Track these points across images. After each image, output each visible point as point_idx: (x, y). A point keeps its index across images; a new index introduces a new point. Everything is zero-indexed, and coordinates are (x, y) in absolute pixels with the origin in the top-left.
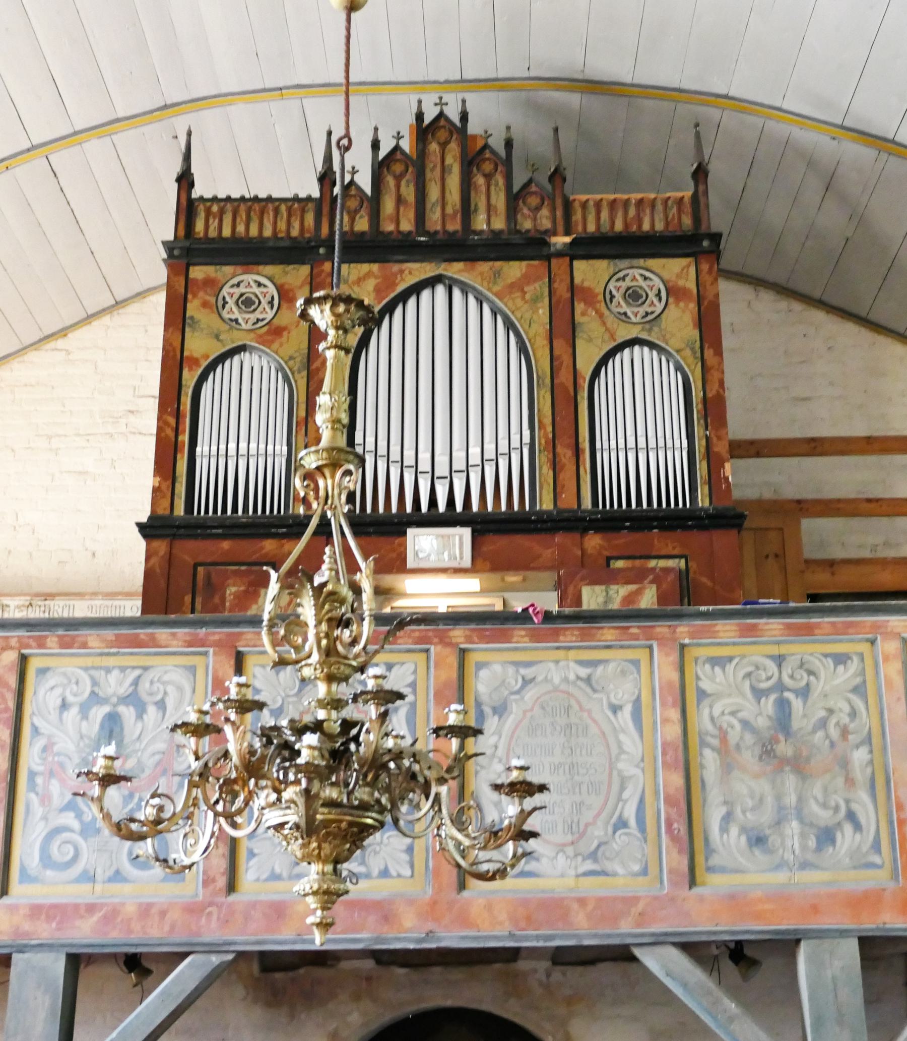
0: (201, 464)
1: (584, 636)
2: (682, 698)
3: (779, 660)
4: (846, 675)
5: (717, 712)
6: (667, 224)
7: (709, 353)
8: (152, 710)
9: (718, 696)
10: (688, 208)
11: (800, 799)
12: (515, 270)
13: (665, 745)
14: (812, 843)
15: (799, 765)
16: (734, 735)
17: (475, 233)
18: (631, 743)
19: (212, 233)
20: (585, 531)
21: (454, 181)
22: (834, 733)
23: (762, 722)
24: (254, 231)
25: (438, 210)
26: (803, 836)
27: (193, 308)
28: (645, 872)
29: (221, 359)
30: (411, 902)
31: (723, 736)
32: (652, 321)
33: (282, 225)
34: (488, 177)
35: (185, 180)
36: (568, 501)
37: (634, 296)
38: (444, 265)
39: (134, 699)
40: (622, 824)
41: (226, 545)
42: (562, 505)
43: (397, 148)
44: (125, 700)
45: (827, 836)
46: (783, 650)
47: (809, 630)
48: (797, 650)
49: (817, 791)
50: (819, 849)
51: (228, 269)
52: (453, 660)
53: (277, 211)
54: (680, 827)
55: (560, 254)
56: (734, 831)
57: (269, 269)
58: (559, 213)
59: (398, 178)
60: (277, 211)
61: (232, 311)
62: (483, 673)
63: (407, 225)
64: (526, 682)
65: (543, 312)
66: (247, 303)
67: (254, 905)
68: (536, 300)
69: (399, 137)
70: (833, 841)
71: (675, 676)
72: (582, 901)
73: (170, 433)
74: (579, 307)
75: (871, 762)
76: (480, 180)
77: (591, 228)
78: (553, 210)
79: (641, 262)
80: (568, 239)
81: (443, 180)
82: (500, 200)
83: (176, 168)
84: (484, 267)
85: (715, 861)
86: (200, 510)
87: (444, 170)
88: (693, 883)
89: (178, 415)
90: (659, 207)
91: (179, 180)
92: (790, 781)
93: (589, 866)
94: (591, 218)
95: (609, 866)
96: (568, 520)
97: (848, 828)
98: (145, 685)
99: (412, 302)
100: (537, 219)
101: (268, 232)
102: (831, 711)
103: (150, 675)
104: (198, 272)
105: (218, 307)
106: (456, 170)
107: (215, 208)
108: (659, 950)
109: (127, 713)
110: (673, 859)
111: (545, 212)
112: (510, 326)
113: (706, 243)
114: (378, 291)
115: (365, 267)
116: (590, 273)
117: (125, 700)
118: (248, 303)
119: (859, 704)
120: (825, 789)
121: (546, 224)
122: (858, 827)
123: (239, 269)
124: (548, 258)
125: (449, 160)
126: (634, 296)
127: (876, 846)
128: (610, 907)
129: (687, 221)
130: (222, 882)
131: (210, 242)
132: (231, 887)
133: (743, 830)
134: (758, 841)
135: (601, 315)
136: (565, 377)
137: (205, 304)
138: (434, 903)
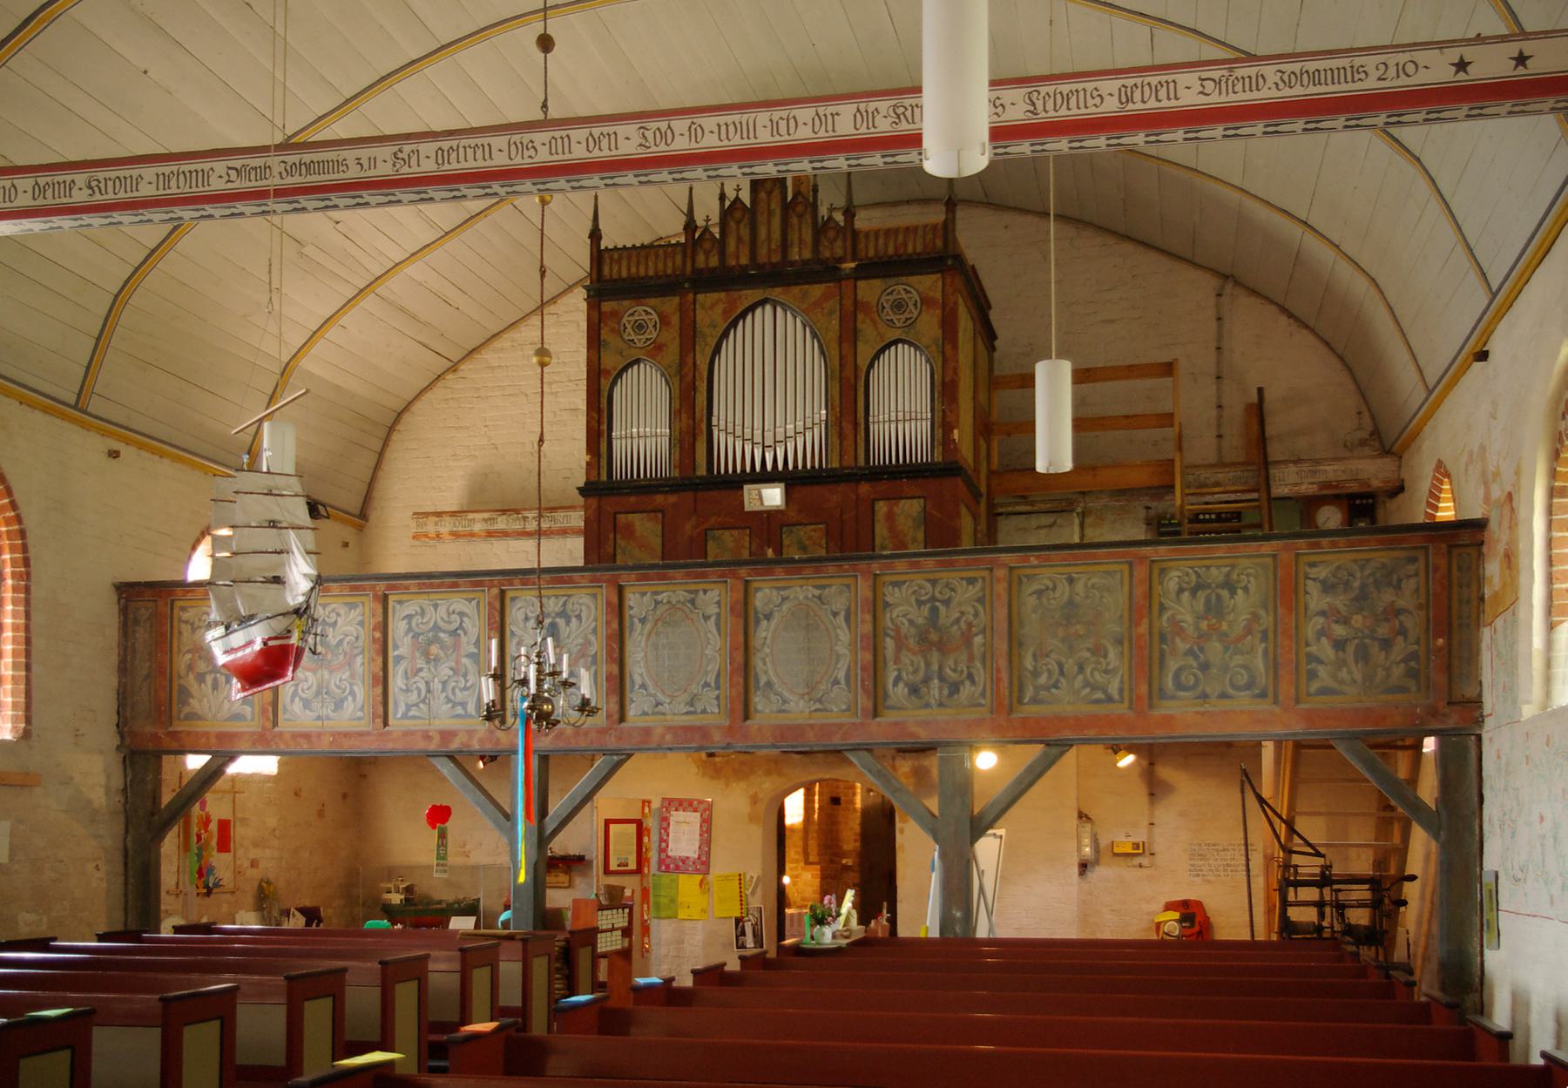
0: (616, 444)
1: (818, 570)
2: (876, 607)
3: (934, 582)
4: (973, 591)
5: (895, 614)
6: (925, 246)
7: (948, 347)
8: (574, 620)
9: (897, 605)
10: (940, 233)
11: (941, 668)
12: (817, 290)
13: (863, 636)
14: (946, 692)
15: (942, 647)
16: (904, 630)
17: (792, 264)
18: (844, 635)
19: (615, 276)
20: (858, 481)
21: (776, 222)
22: (963, 625)
23: (921, 621)
24: (642, 272)
25: (765, 246)
26: (941, 689)
27: (605, 334)
28: (848, 709)
29: (625, 369)
30: (718, 727)
31: (898, 630)
32: (910, 324)
33: (660, 266)
34: (800, 216)
35: (595, 235)
36: (849, 461)
37: (899, 306)
38: (769, 290)
39: (563, 614)
40: (836, 682)
41: (633, 499)
42: (845, 464)
43: (737, 198)
44: (559, 615)
45: (955, 688)
46: (937, 576)
47: (951, 564)
48: (945, 576)
49: (951, 663)
50: (951, 695)
51: (626, 303)
52: (741, 587)
53: (657, 256)
54: (869, 683)
55: (848, 277)
56: (901, 685)
57: (653, 301)
58: (849, 243)
59: (738, 223)
60: (657, 256)
61: (630, 334)
62: (759, 595)
63: (744, 260)
64: (784, 599)
65: (835, 322)
66: (640, 327)
67: (635, 729)
68: (831, 313)
69: (738, 190)
70: (958, 691)
71: (870, 594)
72: (812, 726)
73: (595, 424)
74: (860, 317)
75: (984, 645)
76: (795, 220)
77: (871, 253)
78: (845, 240)
79: (904, 279)
80: (853, 265)
81: (769, 222)
82: (808, 235)
83: (589, 225)
84: (796, 290)
85: (889, 703)
86: (617, 475)
87: (770, 213)
88: (876, 714)
89: (599, 411)
90: (920, 233)
91: (590, 237)
92: (935, 657)
93: (818, 706)
94: (871, 245)
95: (828, 706)
96: (849, 475)
97: (968, 683)
98: (569, 606)
99: (749, 317)
100: (834, 248)
101: (651, 273)
102: (962, 613)
103: (572, 600)
104: (607, 306)
105: (618, 332)
106: (778, 212)
107: (616, 256)
108: (861, 753)
109: (561, 622)
110: (864, 702)
111: (839, 243)
112: (814, 335)
113: (950, 262)
114: (725, 313)
115: (715, 296)
116: (869, 290)
117: (559, 615)
118: (640, 327)
119: (980, 608)
120: (956, 663)
121: (839, 252)
122: (973, 682)
123: (633, 302)
124: (839, 280)
125: (773, 206)
126: (899, 306)
127: (983, 695)
128: (826, 730)
129: (939, 243)
130: (616, 717)
131: (615, 281)
132: (622, 719)
133: (906, 684)
134: (914, 690)
135: (874, 323)
136: (849, 372)
137: (613, 330)
138: (730, 727)
